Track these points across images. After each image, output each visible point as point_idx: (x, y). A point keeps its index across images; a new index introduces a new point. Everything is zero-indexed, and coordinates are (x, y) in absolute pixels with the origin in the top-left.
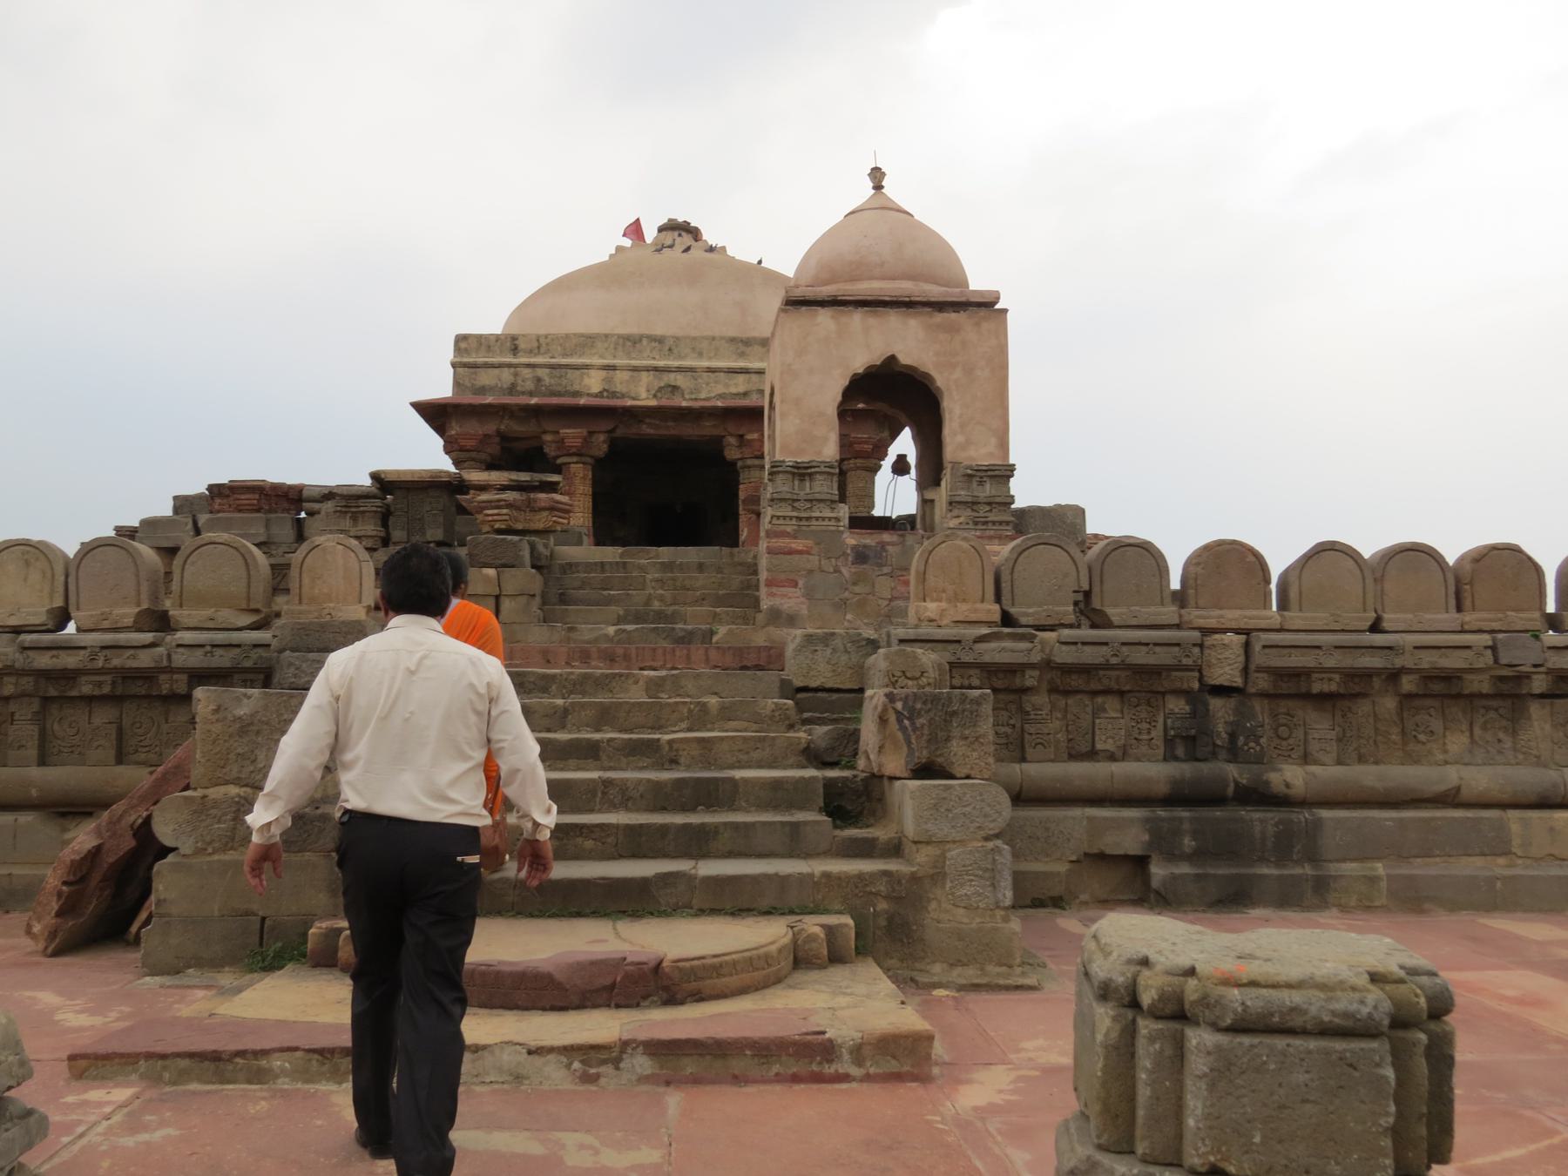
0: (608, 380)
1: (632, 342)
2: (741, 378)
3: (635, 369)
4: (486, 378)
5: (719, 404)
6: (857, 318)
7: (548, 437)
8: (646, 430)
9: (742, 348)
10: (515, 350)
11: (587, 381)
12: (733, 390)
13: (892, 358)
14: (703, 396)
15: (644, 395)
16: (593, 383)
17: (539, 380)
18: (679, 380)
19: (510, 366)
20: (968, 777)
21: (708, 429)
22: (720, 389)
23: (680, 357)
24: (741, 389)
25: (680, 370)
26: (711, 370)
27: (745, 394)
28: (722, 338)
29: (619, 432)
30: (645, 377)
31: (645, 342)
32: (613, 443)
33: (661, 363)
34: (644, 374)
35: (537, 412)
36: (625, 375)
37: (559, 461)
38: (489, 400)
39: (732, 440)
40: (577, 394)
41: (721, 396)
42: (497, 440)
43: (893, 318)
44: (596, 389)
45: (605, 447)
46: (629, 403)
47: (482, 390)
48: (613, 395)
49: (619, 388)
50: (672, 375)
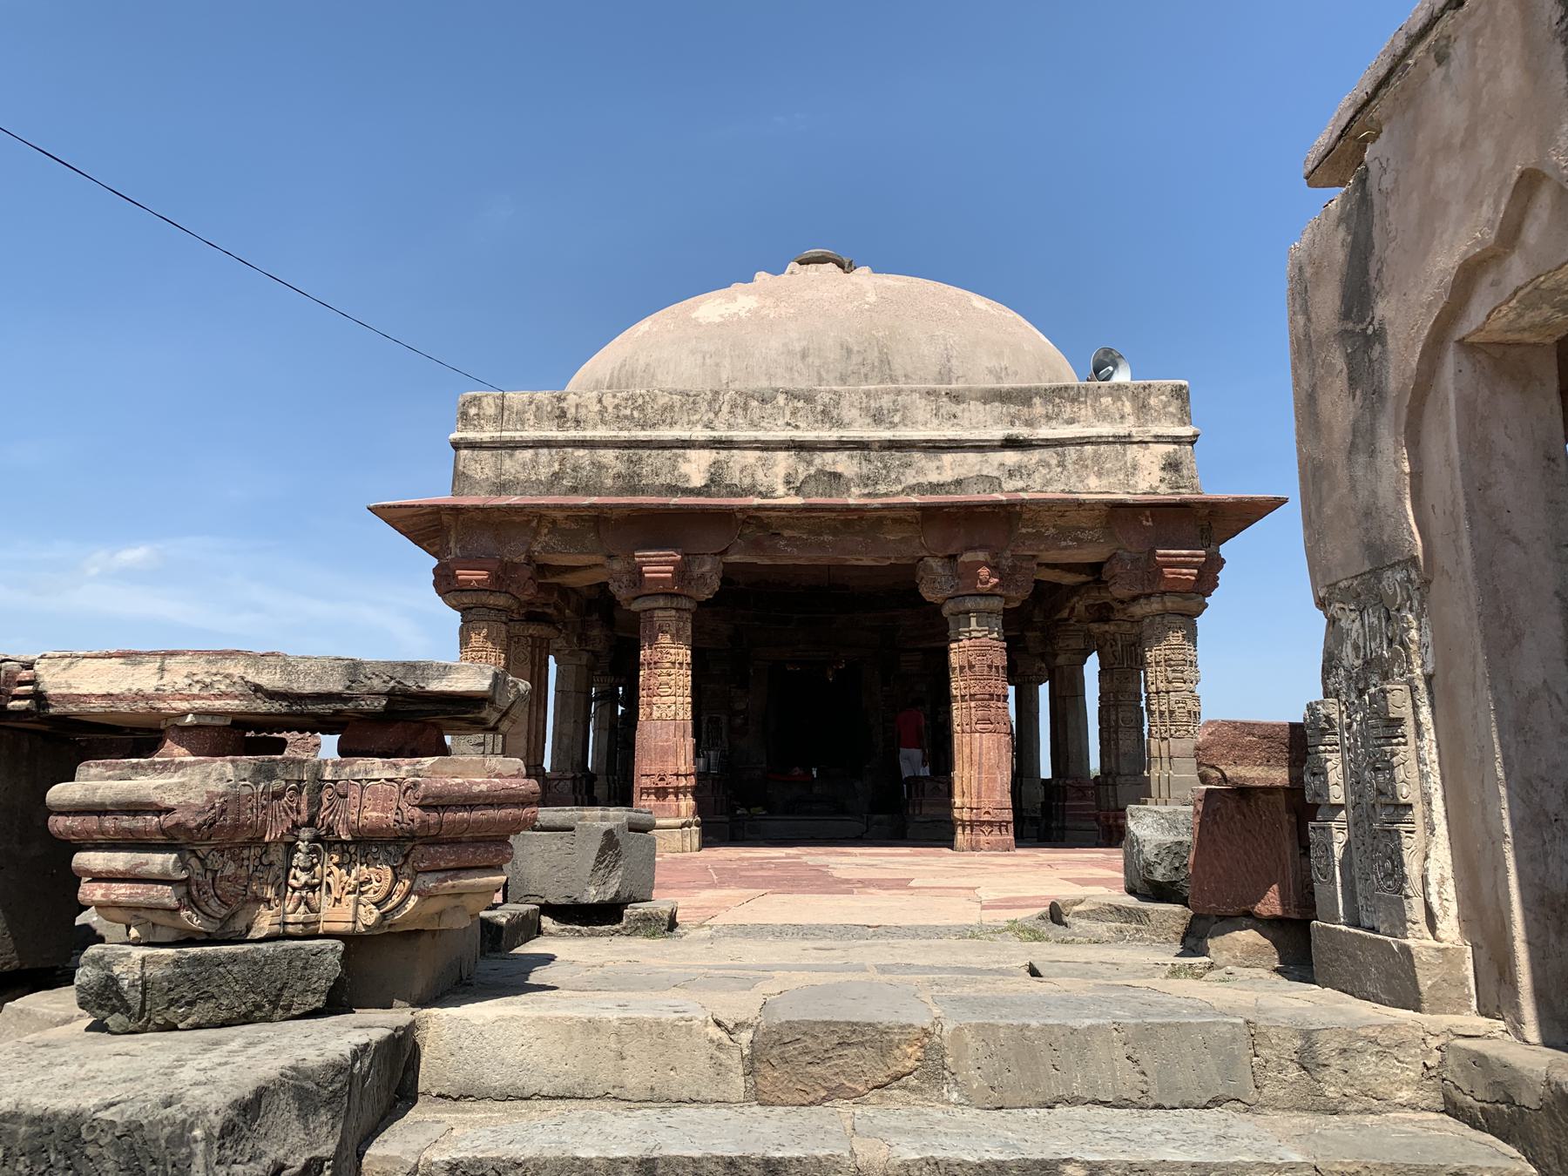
2: (947, 458)
3: (766, 446)
5: (914, 499)
7: (617, 566)
8: (788, 554)
9: (948, 406)
11: (684, 468)
12: (934, 478)
16: (695, 468)
17: (600, 466)
20: (1373, 929)
22: (910, 478)
23: (840, 424)
24: (948, 476)
27: (958, 482)
30: (783, 461)
31: (781, 399)
32: (729, 576)
33: (810, 435)
34: (782, 455)
35: (598, 521)
37: (635, 607)
38: (514, 500)
39: (935, 564)
41: (912, 489)
42: (527, 572)
44: (698, 481)
45: (715, 584)
46: (757, 501)
48: (733, 491)
49: (734, 476)
50: (829, 456)
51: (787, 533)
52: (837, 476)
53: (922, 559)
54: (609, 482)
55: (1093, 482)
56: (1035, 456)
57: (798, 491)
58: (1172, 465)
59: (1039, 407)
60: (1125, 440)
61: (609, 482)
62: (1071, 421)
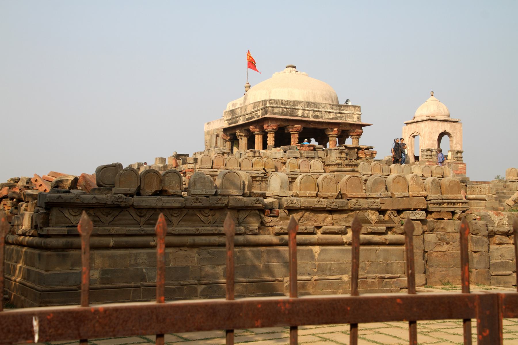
0: (303, 113)
1: (308, 104)
2: (332, 114)
4: (276, 110)
6: (440, 123)
8: (311, 126)
10: (282, 104)
13: (445, 131)
17: (287, 111)
18: (318, 114)
19: (282, 108)
21: (324, 127)
22: (327, 117)
24: (331, 117)
25: (319, 111)
26: (325, 112)
29: (306, 126)
32: (304, 128)
33: (315, 109)
36: (307, 112)
41: (328, 119)
43: (446, 123)
44: (300, 115)
49: (306, 115)
52: (318, 116)
55: (349, 119)
56: (342, 115)
58: (358, 118)
59: (343, 108)
60: (353, 114)
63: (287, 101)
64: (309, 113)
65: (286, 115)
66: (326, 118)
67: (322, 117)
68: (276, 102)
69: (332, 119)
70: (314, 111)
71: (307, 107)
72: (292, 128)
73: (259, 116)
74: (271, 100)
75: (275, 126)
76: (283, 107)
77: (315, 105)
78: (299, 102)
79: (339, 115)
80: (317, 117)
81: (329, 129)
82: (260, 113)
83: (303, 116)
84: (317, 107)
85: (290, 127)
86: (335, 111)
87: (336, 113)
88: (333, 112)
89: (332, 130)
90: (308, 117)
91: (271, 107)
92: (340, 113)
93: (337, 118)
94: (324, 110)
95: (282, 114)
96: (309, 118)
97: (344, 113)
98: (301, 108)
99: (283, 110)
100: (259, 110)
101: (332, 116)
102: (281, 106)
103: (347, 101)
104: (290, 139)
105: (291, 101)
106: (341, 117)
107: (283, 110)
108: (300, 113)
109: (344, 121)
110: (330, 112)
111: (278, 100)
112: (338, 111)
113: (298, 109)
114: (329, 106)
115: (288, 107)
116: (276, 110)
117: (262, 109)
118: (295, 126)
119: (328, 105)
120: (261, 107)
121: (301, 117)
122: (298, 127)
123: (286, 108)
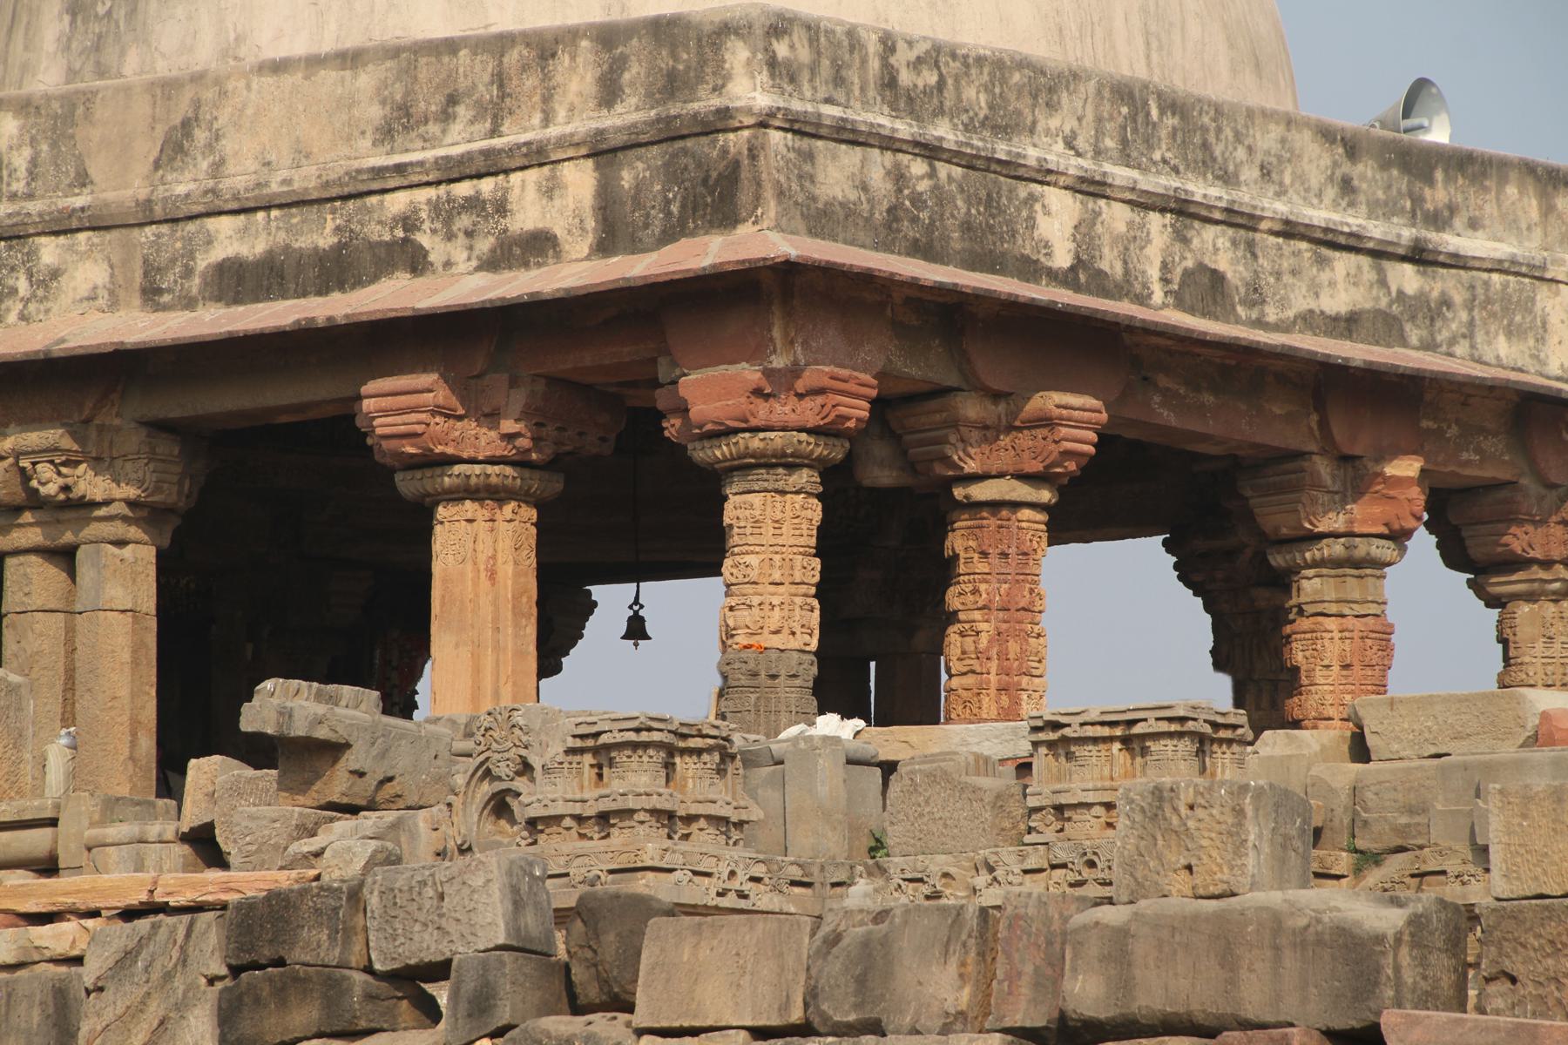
1: (1135, 109)
2: (1343, 263)
4: (839, 174)
14: (1272, 314)
15: (1158, 296)
18: (1215, 247)
19: (889, 143)
22: (1301, 302)
24: (1337, 302)
26: (1290, 230)
28: (1307, 123)
33: (1201, 189)
34: (1155, 221)
36: (1117, 216)
40: (1030, 269)
41: (1308, 320)
44: (1062, 259)
47: (821, 220)
48: (1101, 284)
49: (1110, 262)
51: (1163, 381)
53: (1300, 455)
54: (956, 241)
56: (1446, 283)
57: (1180, 304)
59: (1438, 195)
61: (956, 241)
62: (1474, 224)
63: (935, 56)
64: (1132, 241)
65: (925, 250)
66: (1308, 305)
67: (1256, 295)
68: (835, 51)
69: (1348, 324)
70: (1182, 210)
71: (1126, 159)
72: (990, 432)
73: (540, 245)
74: (779, 26)
75: (838, 383)
76: (904, 129)
77: (1192, 126)
78: (1047, 85)
79: (1407, 278)
80: (1207, 288)
81: (1323, 468)
82: (558, 203)
83: (1082, 272)
84: (1207, 163)
85: (972, 408)
86: (1377, 230)
87: (1380, 254)
88: (1352, 244)
89: (1357, 478)
90: (1121, 290)
91: (799, 127)
92: (1419, 256)
93: (1387, 326)
94: (1276, 207)
95: (887, 234)
96: (1142, 299)
97: (1458, 262)
98: (1074, 166)
99: (899, 177)
100: (537, 156)
101: (1343, 286)
102: (881, 119)
103: (1417, 95)
104: (945, 570)
105: (971, 62)
106: (1432, 311)
107: (899, 177)
108: (1056, 223)
109: (1457, 363)
110: (1330, 241)
111: (853, 38)
112: (1407, 234)
113: (1044, 175)
114: (1316, 160)
115: (944, 132)
116: (839, 174)
117: (603, 152)
118: (1051, 400)
119: (1305, 141)
120: (575, 116)
121: (1067, 278)
122: (1074, 414)
123: (930, 151)
